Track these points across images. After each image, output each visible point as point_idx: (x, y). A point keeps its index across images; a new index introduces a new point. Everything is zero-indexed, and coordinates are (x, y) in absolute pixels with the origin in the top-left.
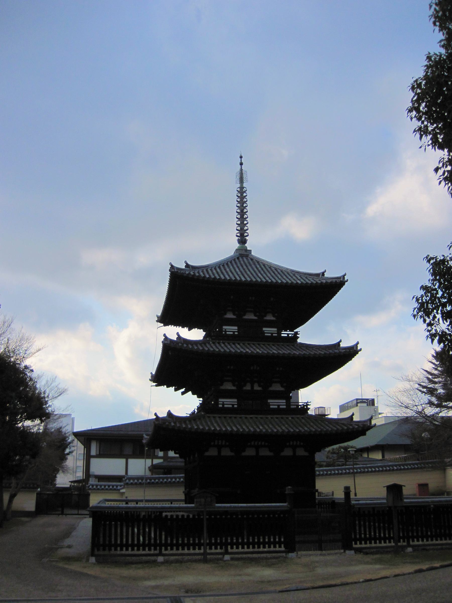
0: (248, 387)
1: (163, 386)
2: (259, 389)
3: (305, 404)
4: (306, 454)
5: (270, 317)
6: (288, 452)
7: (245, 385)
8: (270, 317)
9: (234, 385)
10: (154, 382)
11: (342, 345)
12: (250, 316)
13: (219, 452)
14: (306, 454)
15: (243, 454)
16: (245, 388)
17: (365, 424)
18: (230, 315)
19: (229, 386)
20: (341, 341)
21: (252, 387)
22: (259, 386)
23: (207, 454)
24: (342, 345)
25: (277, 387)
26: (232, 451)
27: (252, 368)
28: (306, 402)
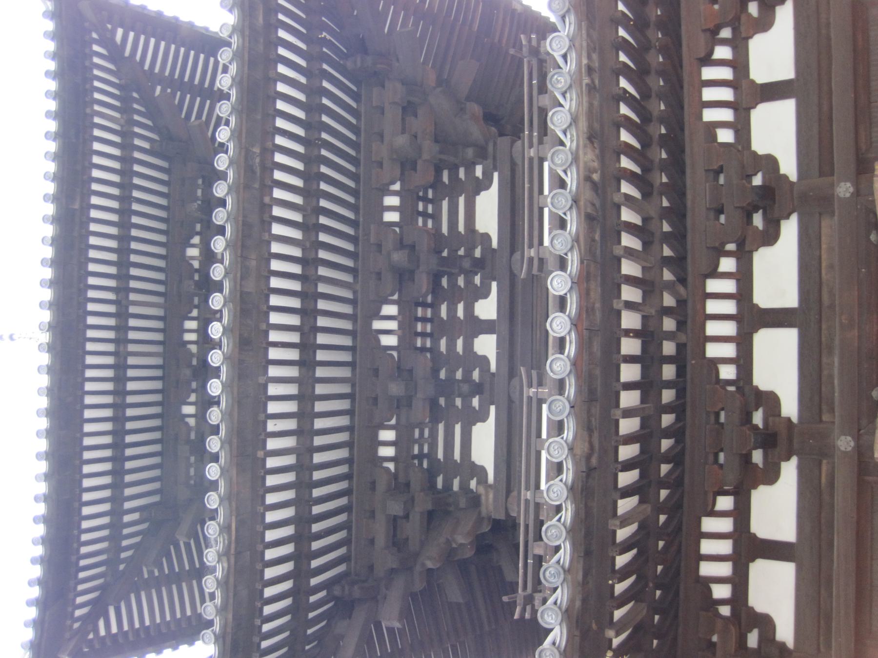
15: (790, 408)
21: (487, 327)
26: (771, 476)
27: (389, 341)
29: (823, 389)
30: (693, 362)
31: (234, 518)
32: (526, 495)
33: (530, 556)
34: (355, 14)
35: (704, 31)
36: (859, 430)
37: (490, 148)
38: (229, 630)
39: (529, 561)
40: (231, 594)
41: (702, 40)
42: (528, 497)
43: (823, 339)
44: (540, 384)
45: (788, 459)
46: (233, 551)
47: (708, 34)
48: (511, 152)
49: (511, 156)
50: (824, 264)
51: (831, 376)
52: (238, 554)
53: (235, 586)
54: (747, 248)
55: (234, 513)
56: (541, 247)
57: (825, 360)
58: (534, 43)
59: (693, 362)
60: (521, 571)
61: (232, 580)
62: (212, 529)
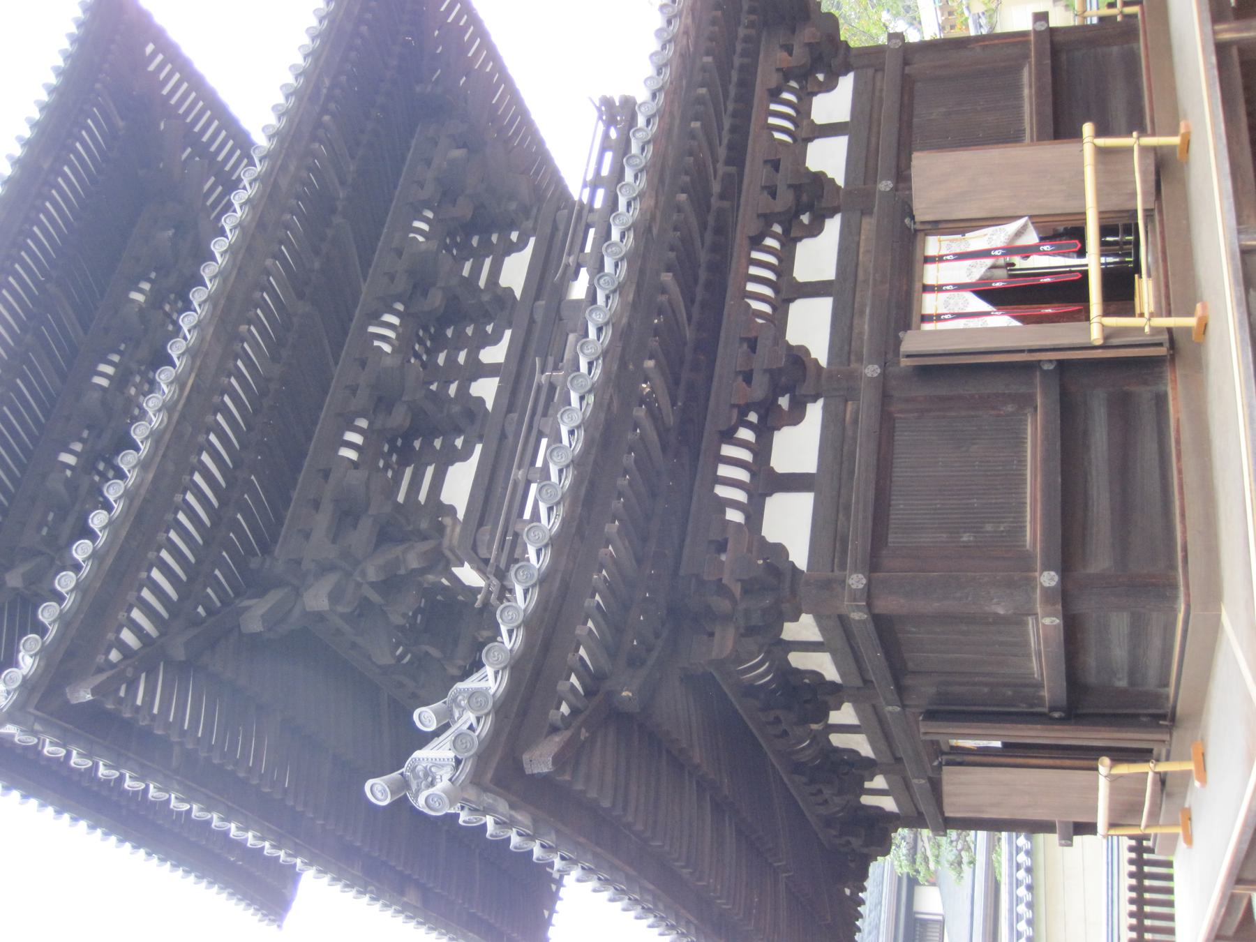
1: (551, 927)
7: (481, 401)
9: (465, 455)
14: (846, 84)
21: (491, 370)
22: (495, 340)
28: (596, 114)
29: (853, 344)
30: (732, 302)
31: (193, 375)
32: (516, 474)
33: (510, 532)
34: (438, 51)
35: (759, 216)
36: (886, 363)
37: (535, 210)
38: (143, 491)
39: (507, 538)
40: (161, 453)
41: (774, 80)
42: (519, 477)
43: (856, 306)
44: (556, 368)
45: (815, 401)
46: (180, 406)
47: (781, 74)
48: (555, 216)
49: (503, 425)
50: (861, 250)
51: (861, 333)
52: (183, 416)
53: (168, 447)
54: (792, 235)
55: (195, 370)
56: (581, 254)
57: (856, 321)
58: (502, 565)
59: (732, 302)
60: (505, 508)
61: (167, 436)
62: (164, 376)
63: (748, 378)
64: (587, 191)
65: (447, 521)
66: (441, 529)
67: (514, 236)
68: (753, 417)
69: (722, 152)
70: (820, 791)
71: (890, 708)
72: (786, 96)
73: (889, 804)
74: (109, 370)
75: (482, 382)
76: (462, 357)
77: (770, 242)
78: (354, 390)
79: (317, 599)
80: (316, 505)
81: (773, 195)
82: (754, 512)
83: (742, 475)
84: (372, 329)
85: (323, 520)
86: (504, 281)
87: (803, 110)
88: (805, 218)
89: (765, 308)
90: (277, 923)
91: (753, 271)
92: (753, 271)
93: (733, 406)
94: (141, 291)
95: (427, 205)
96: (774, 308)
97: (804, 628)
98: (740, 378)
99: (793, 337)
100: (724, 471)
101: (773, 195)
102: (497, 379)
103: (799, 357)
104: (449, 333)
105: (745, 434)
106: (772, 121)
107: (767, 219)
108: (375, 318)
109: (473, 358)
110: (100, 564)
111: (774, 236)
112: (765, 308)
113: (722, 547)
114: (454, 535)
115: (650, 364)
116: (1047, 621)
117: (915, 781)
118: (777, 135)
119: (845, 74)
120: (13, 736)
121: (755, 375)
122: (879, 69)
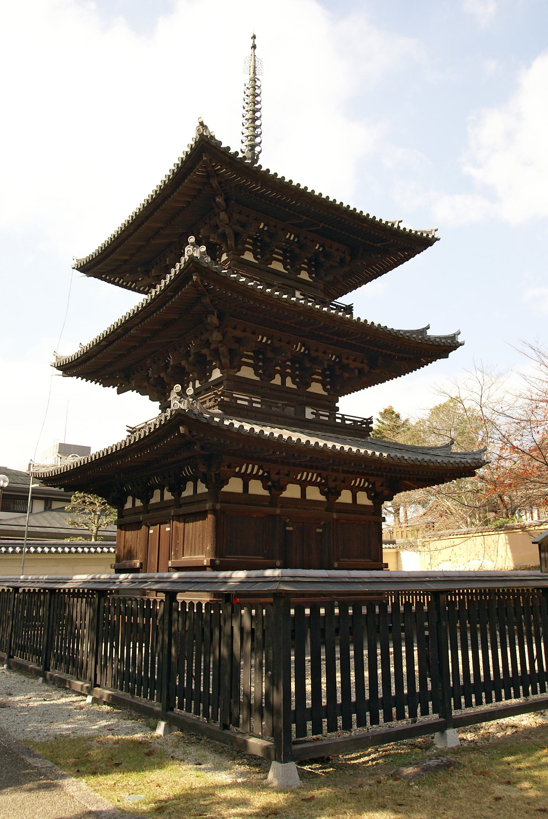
0: (277, 380)
2: (295, 387)
3: (365, 421)
4: (369, 503)
5: (304, 275)
6: (345, 497)
8: (304, 275)
9: (256, 374)
10: (59, 368)
11: (429, 333)
12: (277, 266)
13: (246, 487)
14: (369, 503)
16: (273, 382)
17: (476, 457)
18: (248, 256)
19: (246, 372)
20: (428, 328)
21: (283, 382)
22: (294, 382)
23: (226, 489)
24: (429, 333)
25: (316, 388)
28: (367, 418)
31: (288, 305)
46: (279, 302)
63: (278, 474)
64: (340, 416)
65: (236, 370)
66: (234, 368)
67: (328, 387)
68: (266, 474)
69: (345, 469)
70: (139, 485)
71: (173, 512)
72: (367, 484)
73: (128, 505)
74: (292, 238)
75: (280, 378)
76: (288, 370)
77: (319, 479)
78: (280, 340)
79: (216, 336)
80: (244, 331)
81: (334, 481)
82: (237, 475)
83: (249, 471)
84: (299, 344)
85: (238, 333)
86: (313, 384)
87: (362, 489)
88: (326, 489)
89: (299, 478)
90: (76, 268)
91: (310, 474)
92: (310, 474)
93: (269, 469)
94: (319, 248)
95: (340, 360)
96: (298, 480)
97: (202, 488)
98: (278, 471)
99: (290, 486)
100: (250, 466)
101: (334, 481)
102: (280, 384)
103: (284, 489)
104: (297, 365)
105: (261, 472)
106: (358, 479)
107: (326, 479)
108: (303, 345)
109: (288, 374)
110: (233, 281)
111: (321, 480)
112: (299, 478)
113: (229, 467)
114: (231, 372)
115: (284, 454)
116: (205, 561)
117: (141, 517)
118: (353, 482)
119: (373, 503)
120: (184, 257)
121: (279, 476)
122: (374, 514)
